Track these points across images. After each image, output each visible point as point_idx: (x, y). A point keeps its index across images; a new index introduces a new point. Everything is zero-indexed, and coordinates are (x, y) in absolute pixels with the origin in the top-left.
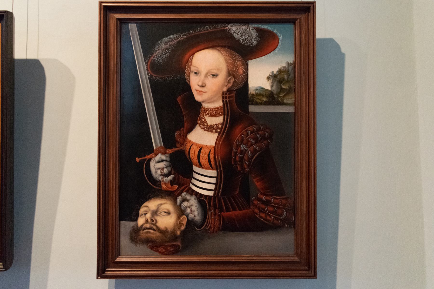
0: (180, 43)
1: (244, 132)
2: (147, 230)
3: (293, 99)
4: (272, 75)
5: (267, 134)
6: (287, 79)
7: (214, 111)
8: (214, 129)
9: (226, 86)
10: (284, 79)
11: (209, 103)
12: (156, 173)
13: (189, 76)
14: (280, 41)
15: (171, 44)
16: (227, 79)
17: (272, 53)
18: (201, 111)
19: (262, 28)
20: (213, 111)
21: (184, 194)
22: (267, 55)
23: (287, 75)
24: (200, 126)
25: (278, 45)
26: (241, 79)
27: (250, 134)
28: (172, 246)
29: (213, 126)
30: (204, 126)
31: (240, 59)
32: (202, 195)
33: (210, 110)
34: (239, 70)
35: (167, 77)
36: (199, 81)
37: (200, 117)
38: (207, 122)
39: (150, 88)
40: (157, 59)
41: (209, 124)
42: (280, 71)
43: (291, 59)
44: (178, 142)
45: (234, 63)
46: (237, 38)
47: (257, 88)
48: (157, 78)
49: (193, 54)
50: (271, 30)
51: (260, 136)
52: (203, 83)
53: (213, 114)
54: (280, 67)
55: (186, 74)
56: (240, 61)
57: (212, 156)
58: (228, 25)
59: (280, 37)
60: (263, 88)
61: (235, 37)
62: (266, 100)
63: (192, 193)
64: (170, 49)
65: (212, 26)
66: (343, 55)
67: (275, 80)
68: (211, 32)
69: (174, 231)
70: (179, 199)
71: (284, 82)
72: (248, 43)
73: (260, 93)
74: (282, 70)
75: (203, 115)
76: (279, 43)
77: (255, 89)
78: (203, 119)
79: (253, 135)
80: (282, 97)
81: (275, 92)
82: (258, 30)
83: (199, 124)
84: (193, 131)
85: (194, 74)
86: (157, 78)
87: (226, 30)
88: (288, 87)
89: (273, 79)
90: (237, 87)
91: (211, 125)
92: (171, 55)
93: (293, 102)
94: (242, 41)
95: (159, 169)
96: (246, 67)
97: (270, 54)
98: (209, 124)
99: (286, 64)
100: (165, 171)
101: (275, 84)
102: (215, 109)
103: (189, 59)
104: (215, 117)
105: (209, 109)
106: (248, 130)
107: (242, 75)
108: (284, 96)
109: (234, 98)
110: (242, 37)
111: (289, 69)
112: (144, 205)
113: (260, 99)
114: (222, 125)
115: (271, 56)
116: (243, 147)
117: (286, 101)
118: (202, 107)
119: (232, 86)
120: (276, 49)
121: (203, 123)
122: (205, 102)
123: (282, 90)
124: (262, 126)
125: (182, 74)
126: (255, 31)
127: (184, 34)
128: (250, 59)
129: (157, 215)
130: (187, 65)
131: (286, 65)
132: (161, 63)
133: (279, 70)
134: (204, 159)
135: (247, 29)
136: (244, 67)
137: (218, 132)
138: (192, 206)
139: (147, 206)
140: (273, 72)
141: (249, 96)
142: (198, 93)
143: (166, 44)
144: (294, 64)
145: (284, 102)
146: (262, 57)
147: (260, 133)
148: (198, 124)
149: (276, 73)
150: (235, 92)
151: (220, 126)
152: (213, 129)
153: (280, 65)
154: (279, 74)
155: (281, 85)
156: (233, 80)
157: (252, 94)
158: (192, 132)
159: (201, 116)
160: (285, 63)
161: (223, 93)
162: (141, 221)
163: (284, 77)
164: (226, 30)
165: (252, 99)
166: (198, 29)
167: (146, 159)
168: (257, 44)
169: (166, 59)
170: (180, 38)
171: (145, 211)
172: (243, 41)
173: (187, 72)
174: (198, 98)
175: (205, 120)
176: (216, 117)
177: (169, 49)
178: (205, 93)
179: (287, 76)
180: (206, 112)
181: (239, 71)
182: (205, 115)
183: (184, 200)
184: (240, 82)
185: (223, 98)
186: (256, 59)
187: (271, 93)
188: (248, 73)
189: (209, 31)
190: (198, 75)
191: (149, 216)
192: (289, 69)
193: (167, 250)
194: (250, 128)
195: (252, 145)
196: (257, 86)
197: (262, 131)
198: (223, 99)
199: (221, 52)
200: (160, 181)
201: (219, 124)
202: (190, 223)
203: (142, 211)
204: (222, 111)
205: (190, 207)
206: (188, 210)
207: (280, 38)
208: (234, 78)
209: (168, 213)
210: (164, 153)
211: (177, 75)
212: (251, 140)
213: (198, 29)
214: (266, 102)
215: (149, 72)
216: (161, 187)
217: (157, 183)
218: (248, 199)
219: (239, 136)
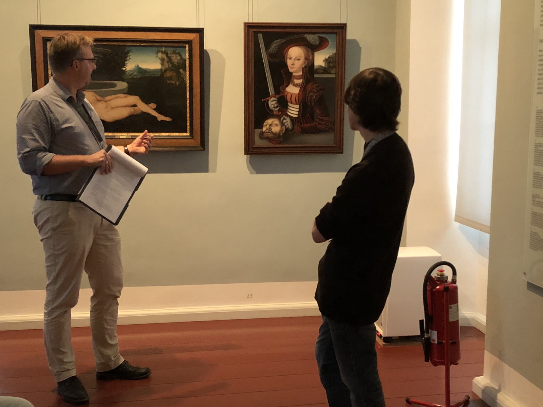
0: (283, 44)
2: (267, 133)
3: (335, 71)
8: (298, 85)
12: (271, 107)
13: (287, 60)
16: (304, 61)
21: (284, 116)
26: (311, 62)
28: (278, 140)
32: (292, 117)
41: (296, 83)
42: (329, 57)
43: (334, 52)
44: (282, 92)
52: (293, 63)
57: (297, 98)
63: (288, 116)
66: (361, 48)
69: (279, 133)
70: (282, 119)
81: (327, 68)
82: (319, 37)
95: (272, 104)
98: (296, 83)
100: (276, 105)
101: (327, 64)
108: (331, 70)
112: (266, 121)
116: (311, 94)
123: (331, 67)
129: (272, 126)
138: (287, 122)
139: (267, 122)
140: (326, 58)
150: (308, 68)
151: (301, 84)
161: (303, 68)
162: (264, 129)
167: (266, 100)
171: (266, 124)
174: (291, 70)
183: (284, 119)
187: (325, 68)
191: (268, 126)
193: (276, 142)
195: (315, 93)
200: (273, 110)
201: (300, 83)
202: (287, 129)
203: (264, 124)
204: (302, 77)
206: (286, 124)
209: (277, 125)
210: (275, 97)
216: (273, 113)
217: (272, 111)
218: (313, 119)
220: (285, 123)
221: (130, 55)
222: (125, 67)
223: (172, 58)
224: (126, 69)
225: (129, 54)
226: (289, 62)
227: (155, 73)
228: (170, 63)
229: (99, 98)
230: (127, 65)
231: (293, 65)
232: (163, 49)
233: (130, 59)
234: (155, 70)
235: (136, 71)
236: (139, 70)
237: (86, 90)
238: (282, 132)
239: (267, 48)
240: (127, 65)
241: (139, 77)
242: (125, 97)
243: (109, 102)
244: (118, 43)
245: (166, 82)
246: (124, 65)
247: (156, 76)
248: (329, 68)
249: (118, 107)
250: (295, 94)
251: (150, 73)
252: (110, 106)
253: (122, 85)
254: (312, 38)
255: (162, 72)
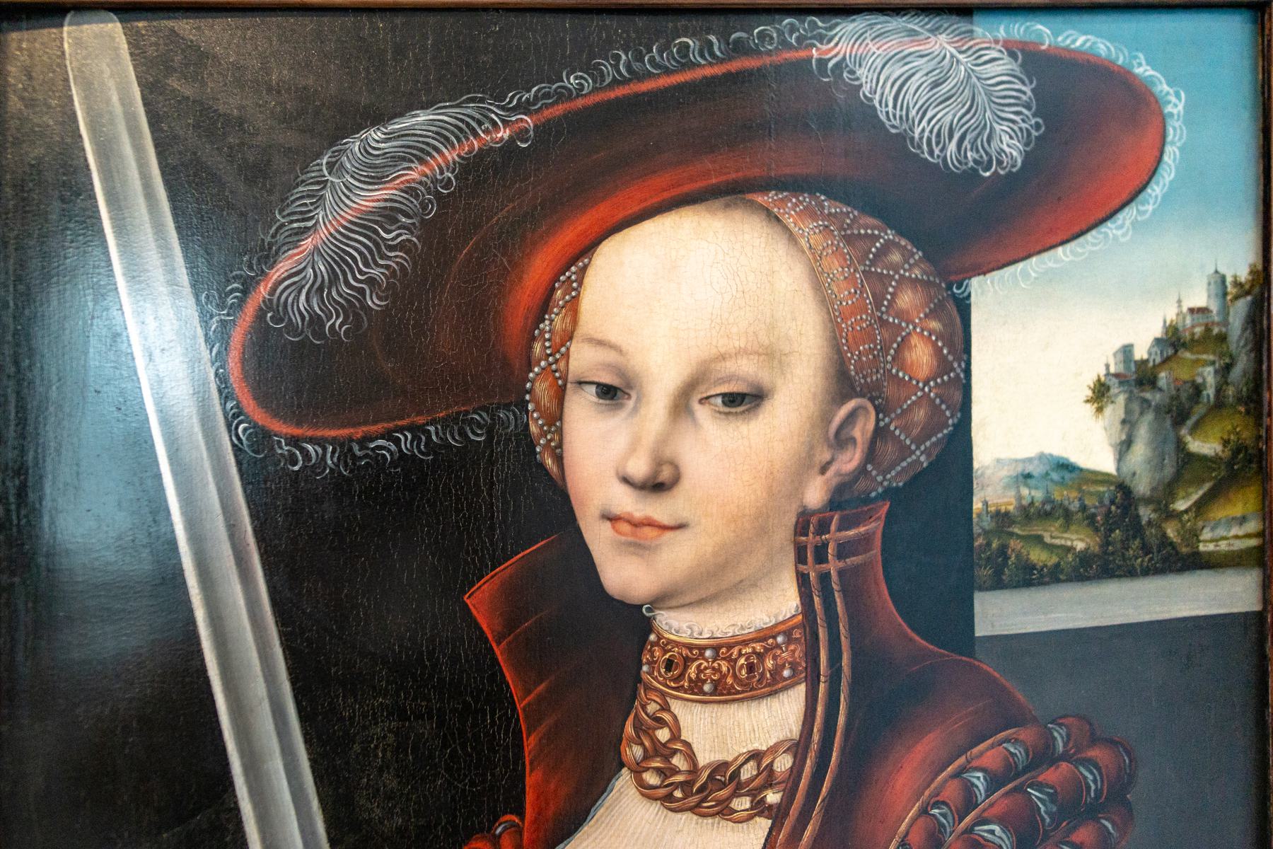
1: (945, 781)
4: (1121, 369)
5: (1095, 781)
6: (1219, 391)
7: (742, 661)
9: (823, 470)
10: (1198, 389)
11: (701, 602)
13: (555, 418)
14: (1176, 134)
15: (414, 175)
16: (826, 419)
17: (1120, 222)
18: (645, 668)
19: (1057, 48)
20: (736, 661)
22: (1094, 232)
23: (1213, 363)
24: (641, 784)
25: (1159, 160)
26: (920, 415)
27: (986, 791)
29: (737, 773)
30: (666, 777)
31: (917, 273)
33: (708, 653)
34: (910, 348)
35: (388, 436)
36: (633, 448)
37: (636, 715)
38: (688, 745)
39: (249, 529)
40: (303, 297)
41: (705, 758)
45: (878, 303)
46: (897, 123)
47: (1029, 468)
48: (310, 447)
49: (588, 248)
50: (1118, 58)
51: (1053, 798)
52: (659, 462)
53: (735, 676)
54: (1171, 314)
55: (537, 404)
56: (914, 282)
58: (831, 28)
59: (1176, 106)
60: (1065, 466)
61: (883, 117)
62: (1087, 549)
64: (407, 216)
65: (724, 37)
67: (1145, 401)
68: (714, 77)
71: (1199, 411)
72: (969, 154)
73: (1048, 500)
74: (1187, 335)
75: (663, 694)
76: (1169, 149)
77: (1017, 477)
78: (661, 723)
79: (1007, 794)
80: (1186, 517)
81: (1142, 487)
83: (632, 771)
84: (585, 828)
85: (595, 399)
86: (310, 447)
87: (822, 63)
88: (1226, 443)
89: (1129, 401)
90: (899, 468)
91: (722, 766)
92: (415, 264)
93: (1253, 542)
94: (929, 140)
96: (958, 320)
97: (1110, 228)
98: (705, 758)
99: (1208, 290)
101: (1143, 432)
102: (745, 643)
103: (553, 290)
104: (752, 698)
105: (702, 649)
106: (974, 764)
107: (926, 383)
108: (1200, 507)
109: (876, 551)
110: (929, 115)
111: (1225, 323)
113: (1048, 540)
114: (795, 757)
115: (1115, 238)
117: (1211, 541)
118: (652, 637)
119: (865, 466)
120: (1149, 190)
121: (662, 755)
122: (674, 603)
124: (1060, 725)
125: (507, 407)
126: (1014, 66)
127: (513, 98)
128: (983, 270)
130: (542, 332)
131: (1209, 296)
132: (339, 335)
133: (1167, 333)
135: (961, 57)
136: (944, 326)
137: (771, 806)
140: (1127, 350)
141: (976, 530)
142: (623, 538)
143: (377, 180)
144: (1257, 290)
145: (1202, 548)
146: (1060, 250)
147: (1051, 775)
148: (625, 771)
149: (1145, 356)
151: (783, 763)
152: (735, 794)
153: (1176, 299)
154: (1166, 361)
155: (1184, 431)
156: (871, 426)
157: (998, 513)
158: (579, 835)
159: (644, 707)
160: (1205, 281)
161: (802, 526)
163: (1199, 380)
164: (822, 63)
165: (995, 545)
166: (618, 58)
168: (1023, 162)
169: (380, 298)
170: (487, 132)
172: (938, 144)
173: (542, 390)
175: (676, 736)
176: (754, 704)
177: (397, 221)
178: (669, 535)
179: (1216, 372)
180: (682, 675)
181: (907, 354)
182: (677, 698)
184: (915, 432)
185: (801, 558)
186: (1020, 266)
188: (968, 363)
189: (698, 74)
190: (619, 406)
192: (1231, 319)
194: (981, 754)
196: (1029, 451)
197: (1064, 765)
198: (801, 567)
199: (786, 228)
201: (773, 750)
204: (799, 651)
207: (1171, 115)
208: (878, 410)
211: (467, 413)
212: (992, 832)
213: (624, 57)
214: (1085, 559)
215: (237, 406)
219: (914, 820)
248: (1169, 490)
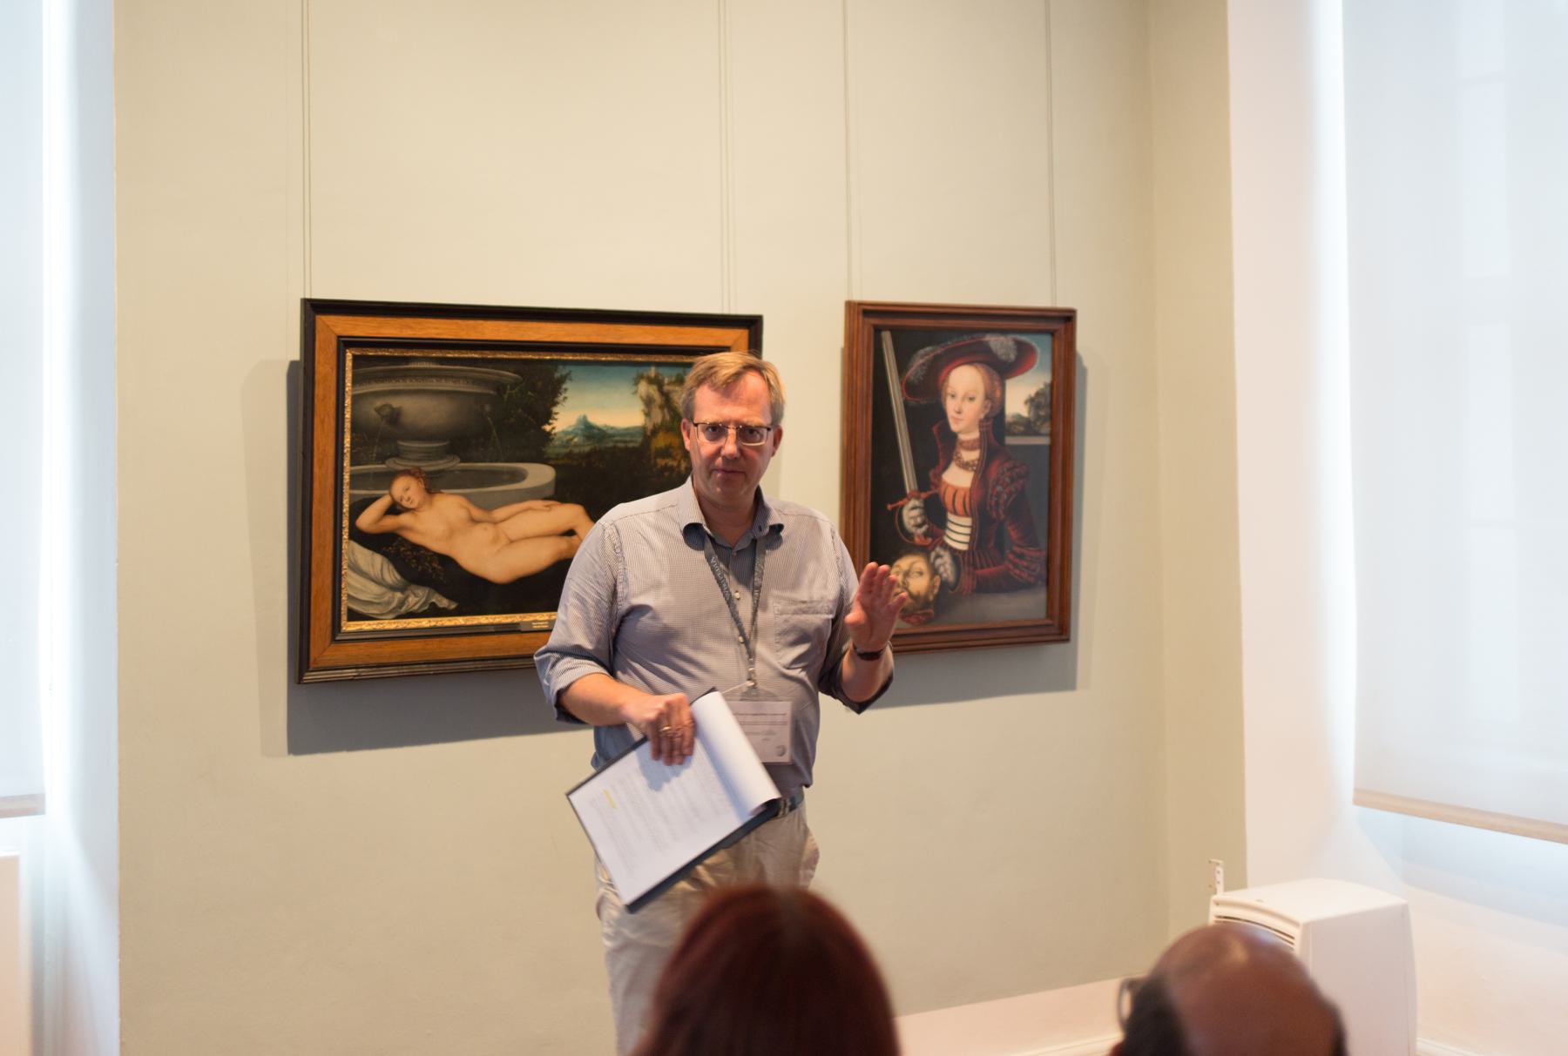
0: (936, 358)
12: (909, 523)
21: (938, 549)
57: (967, 500)
69: (926, 596)
70: (933, 555)
82: (1019, 344)
100: (919, 520)
116: (999, 488)
134: (959, 507)
174: (954, 427)
183: (938, 556)
202: (944, 584)
205: (943, 565)
206: (942, 569)
209: (921, 573)
210: (918, 498)
217: (909, 535)
220: (941, 565)
221: (566, 390)
222: (551, 421)
223: (671, 396)
224: (553, 428)
225: (564, 386)
226: (951, 406)
227: (628, 439)
228: (669, 412)
229: (477, 513)
230: (556, 417)
231: (959, 412)
232: (652, 371)
233: (565, 398)
234: (627, 429)
235: (580, 432)
236: (590, 431)
237: (442, 491)
238: (932, 592)
239: (902, 369)
240: (556, 417)
241: (587, 449)
242: (548, 508)
243: (504, 525)
244: (551, 355)
245: (656, 464)
246: (548, 416)
247: (630, 445)
249: (527, 538)
250: (963, 489)
251: (616, 438)
252: (506, 535)
253: (540, 474)
254: (1000, 344)
255: (647, 435)
